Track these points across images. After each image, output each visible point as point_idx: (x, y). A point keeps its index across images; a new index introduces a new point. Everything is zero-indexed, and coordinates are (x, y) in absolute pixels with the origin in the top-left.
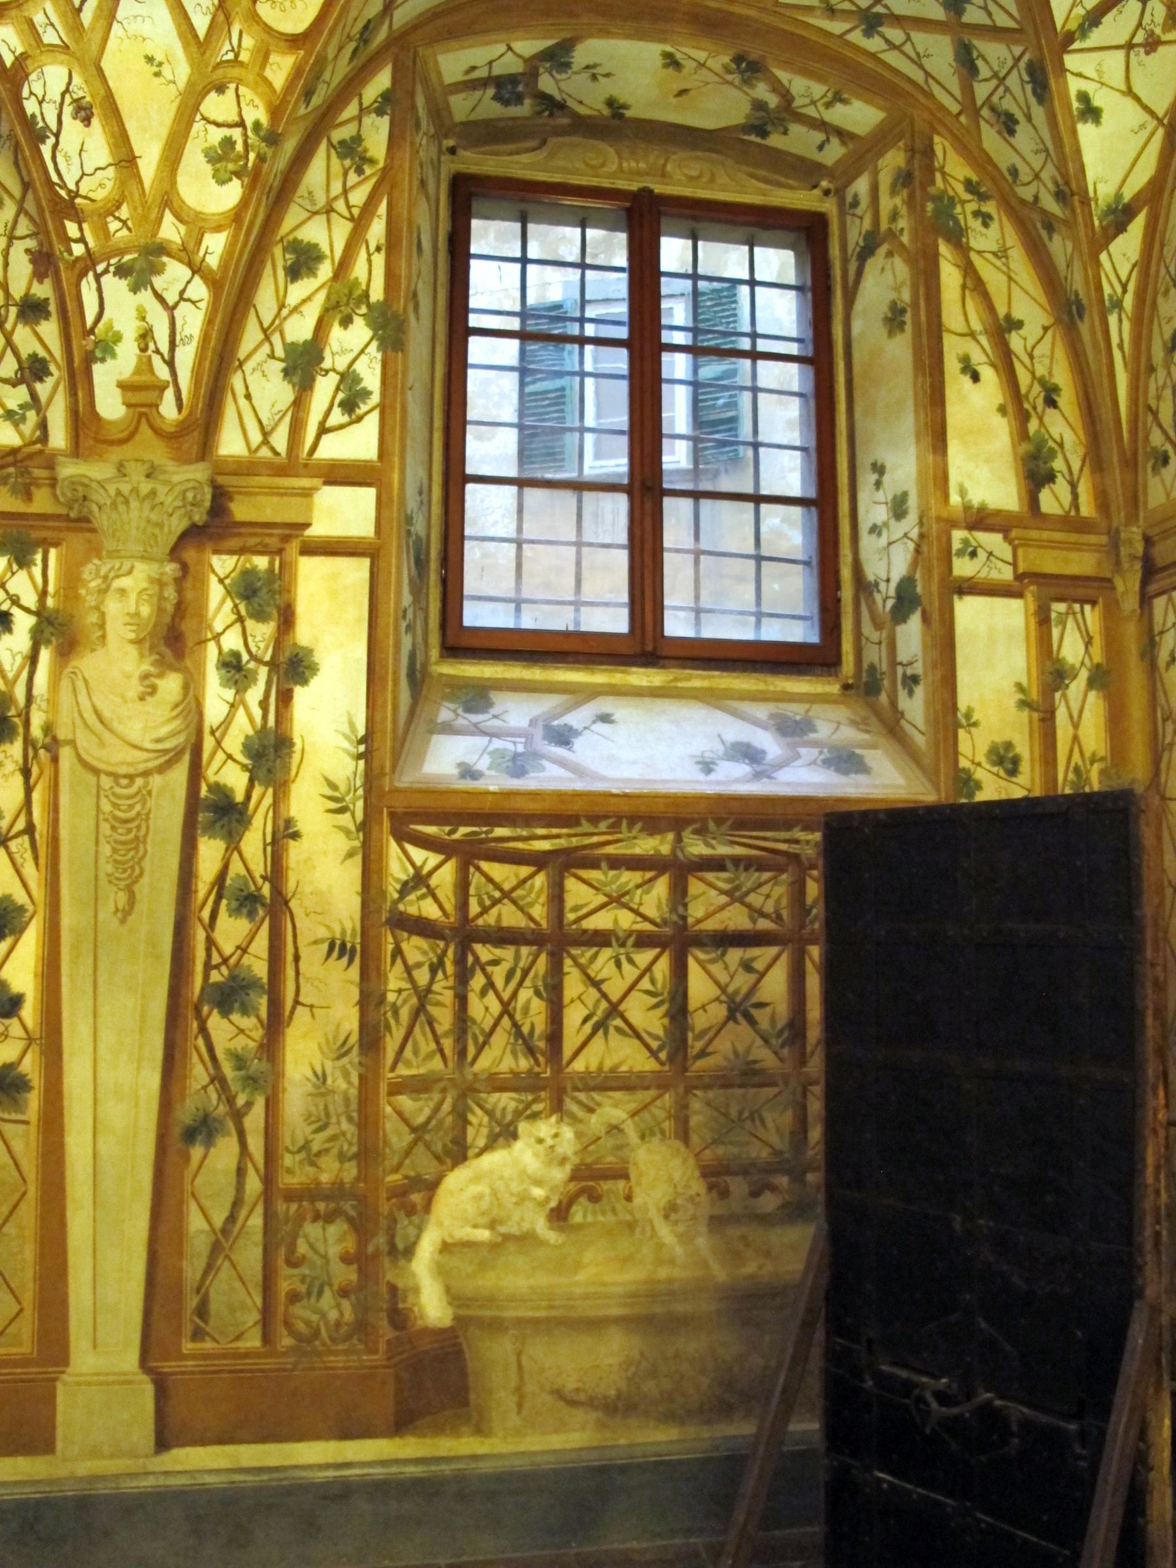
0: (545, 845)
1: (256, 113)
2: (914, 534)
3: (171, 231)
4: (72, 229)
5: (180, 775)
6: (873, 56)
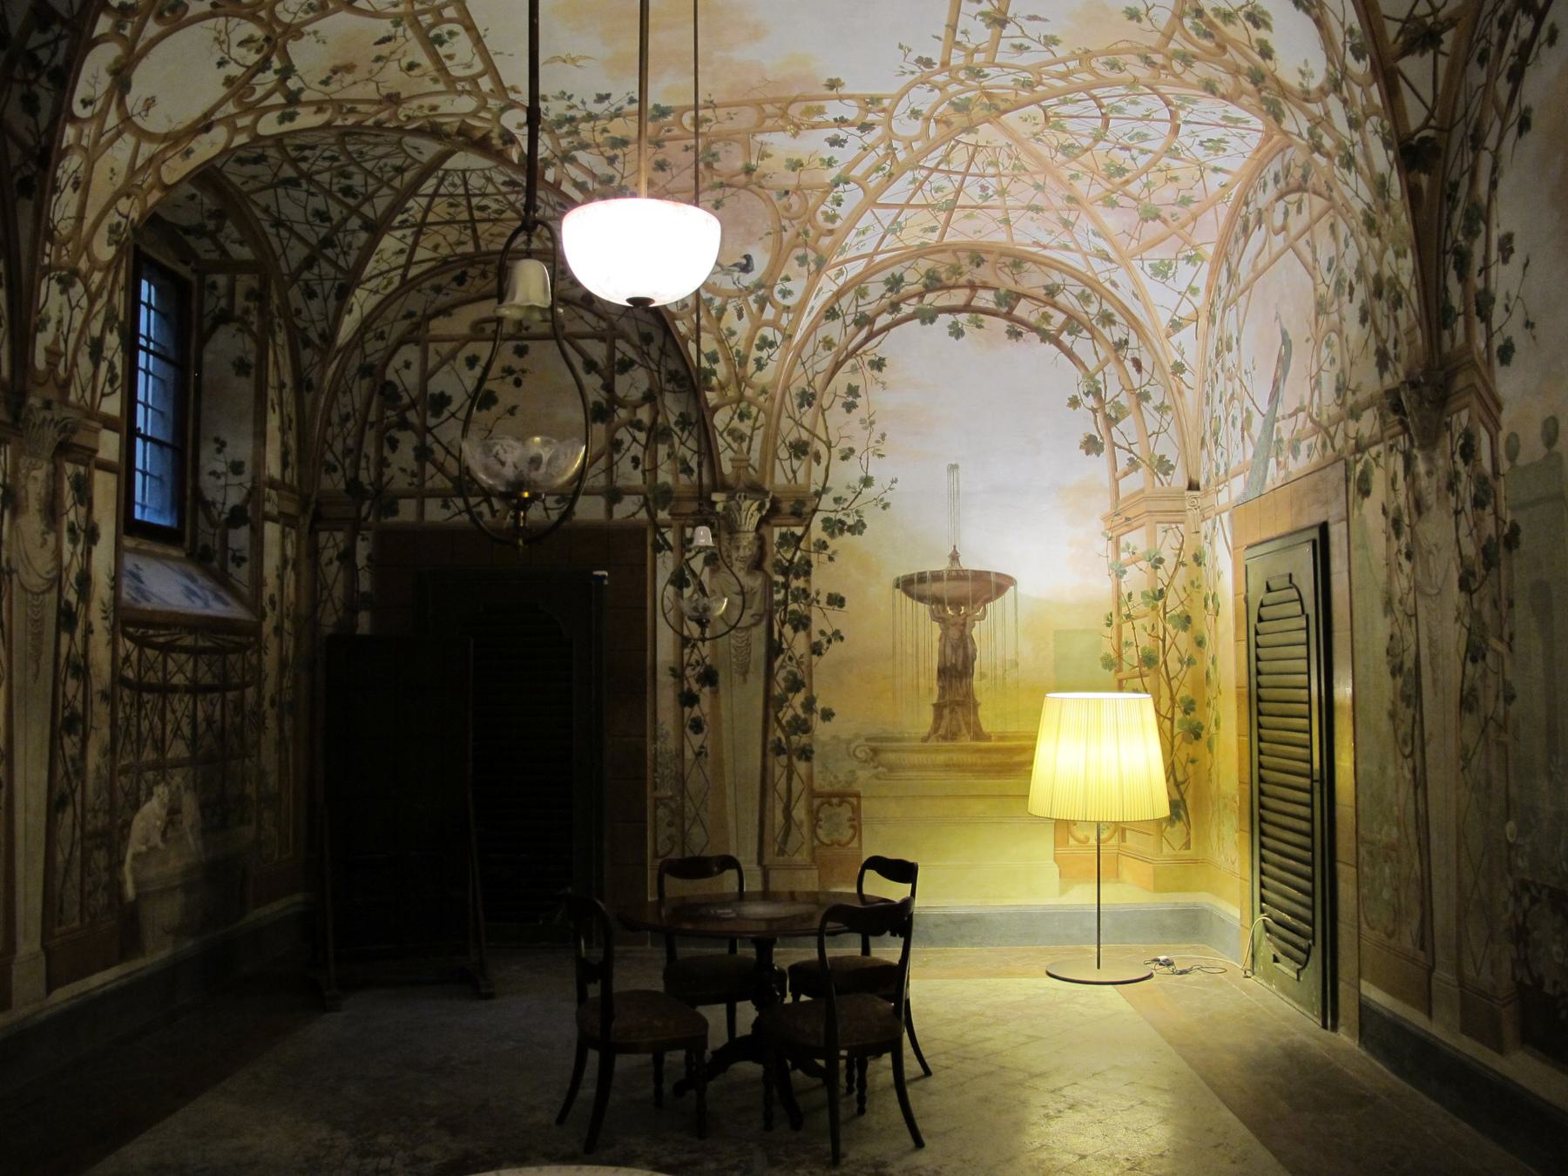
0: (161, 640)
1: (135, 215)
2: (249, 485)
3: (83, 265)
4: (48, 246)
5: (54, 594)
6: (264, 233)
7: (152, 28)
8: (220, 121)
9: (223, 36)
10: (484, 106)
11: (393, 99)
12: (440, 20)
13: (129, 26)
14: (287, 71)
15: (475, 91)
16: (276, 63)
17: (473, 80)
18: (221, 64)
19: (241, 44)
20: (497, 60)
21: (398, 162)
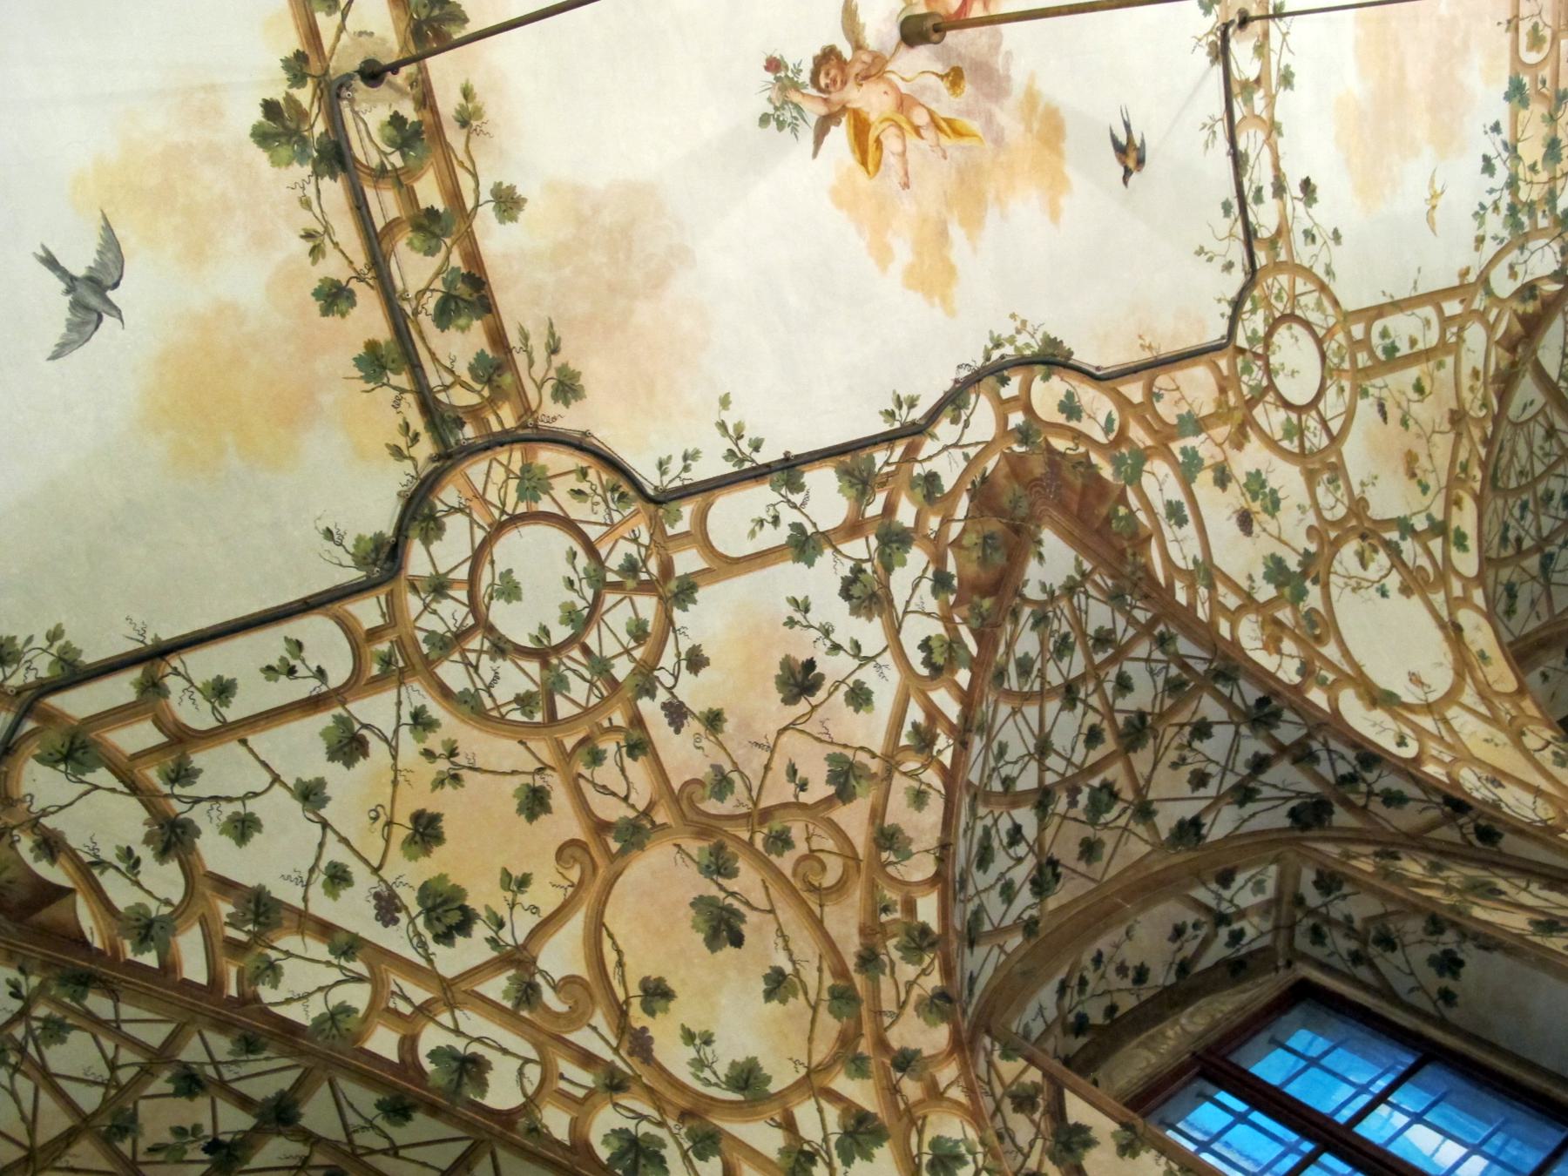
1: (1548, 734)
7: (1330, 650)
8: (1450, 614)
9: (1353, 582)
10: (1482, 316)
11: (1457, 418)
12: (1365, 343)
13: (1323, 673)
14: (1404, 526)
15: (1461, 321)
16: (1393, 535)
17: (1445, 321)
18: (1384, 594)
19: (1364, 566)
20: (1421, 291)
21: (1539, 432)
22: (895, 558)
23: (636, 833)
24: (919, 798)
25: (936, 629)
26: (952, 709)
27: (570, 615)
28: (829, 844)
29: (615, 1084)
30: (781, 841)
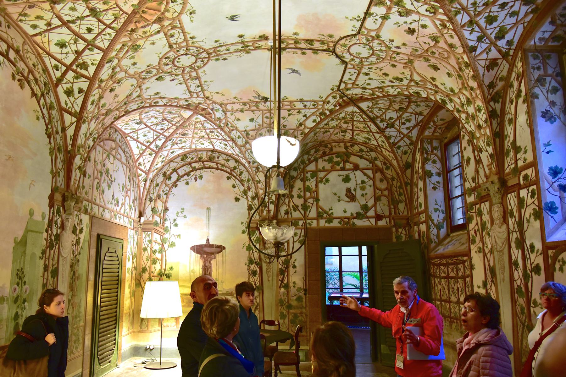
22: (403, 4)
23: (411, 62)
24: (451, 36)
25: (426, 7)
26: (445, 18)
27: (369, 50)
28: (441, 50)
29: (437, 92)
30: (433, 53)
